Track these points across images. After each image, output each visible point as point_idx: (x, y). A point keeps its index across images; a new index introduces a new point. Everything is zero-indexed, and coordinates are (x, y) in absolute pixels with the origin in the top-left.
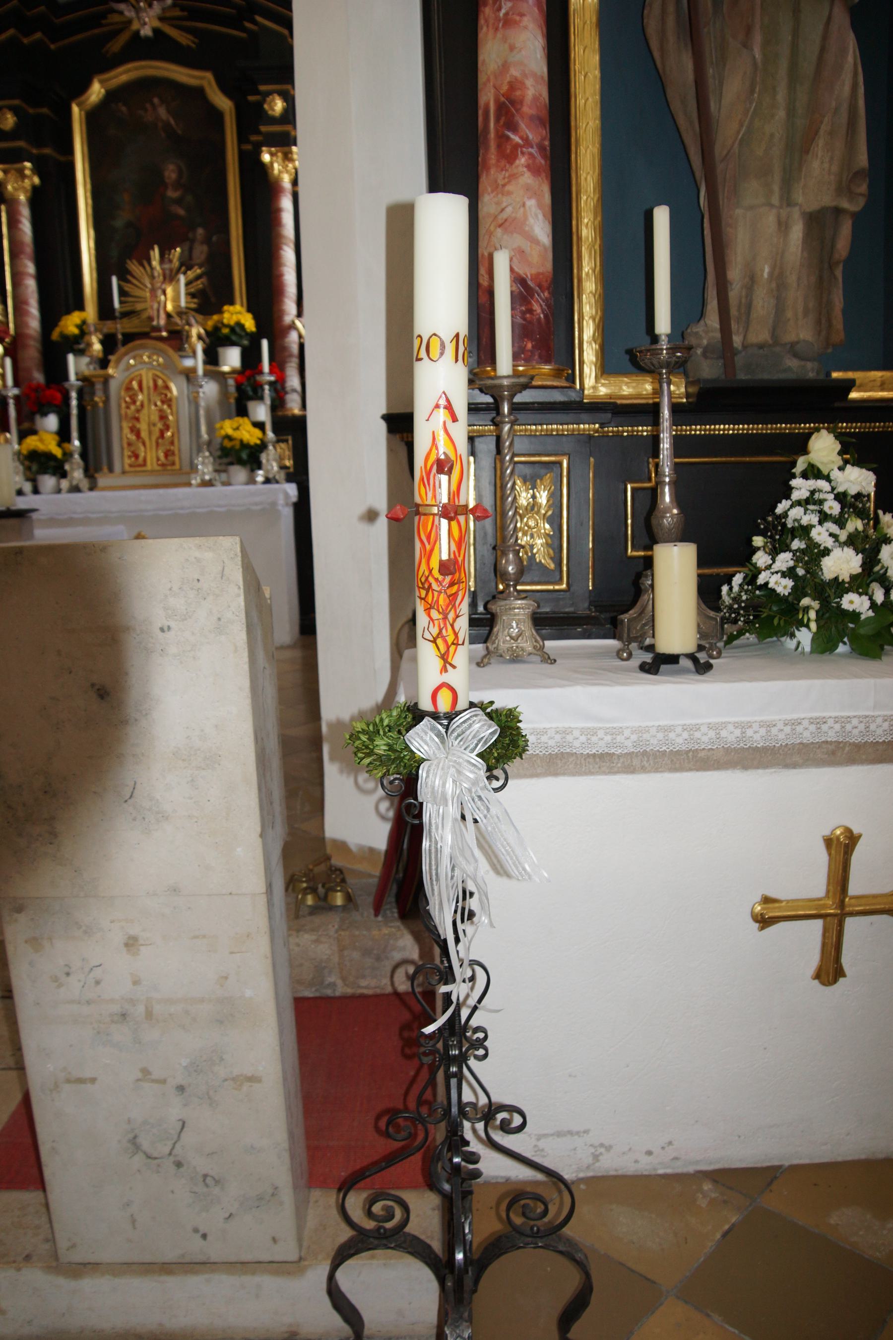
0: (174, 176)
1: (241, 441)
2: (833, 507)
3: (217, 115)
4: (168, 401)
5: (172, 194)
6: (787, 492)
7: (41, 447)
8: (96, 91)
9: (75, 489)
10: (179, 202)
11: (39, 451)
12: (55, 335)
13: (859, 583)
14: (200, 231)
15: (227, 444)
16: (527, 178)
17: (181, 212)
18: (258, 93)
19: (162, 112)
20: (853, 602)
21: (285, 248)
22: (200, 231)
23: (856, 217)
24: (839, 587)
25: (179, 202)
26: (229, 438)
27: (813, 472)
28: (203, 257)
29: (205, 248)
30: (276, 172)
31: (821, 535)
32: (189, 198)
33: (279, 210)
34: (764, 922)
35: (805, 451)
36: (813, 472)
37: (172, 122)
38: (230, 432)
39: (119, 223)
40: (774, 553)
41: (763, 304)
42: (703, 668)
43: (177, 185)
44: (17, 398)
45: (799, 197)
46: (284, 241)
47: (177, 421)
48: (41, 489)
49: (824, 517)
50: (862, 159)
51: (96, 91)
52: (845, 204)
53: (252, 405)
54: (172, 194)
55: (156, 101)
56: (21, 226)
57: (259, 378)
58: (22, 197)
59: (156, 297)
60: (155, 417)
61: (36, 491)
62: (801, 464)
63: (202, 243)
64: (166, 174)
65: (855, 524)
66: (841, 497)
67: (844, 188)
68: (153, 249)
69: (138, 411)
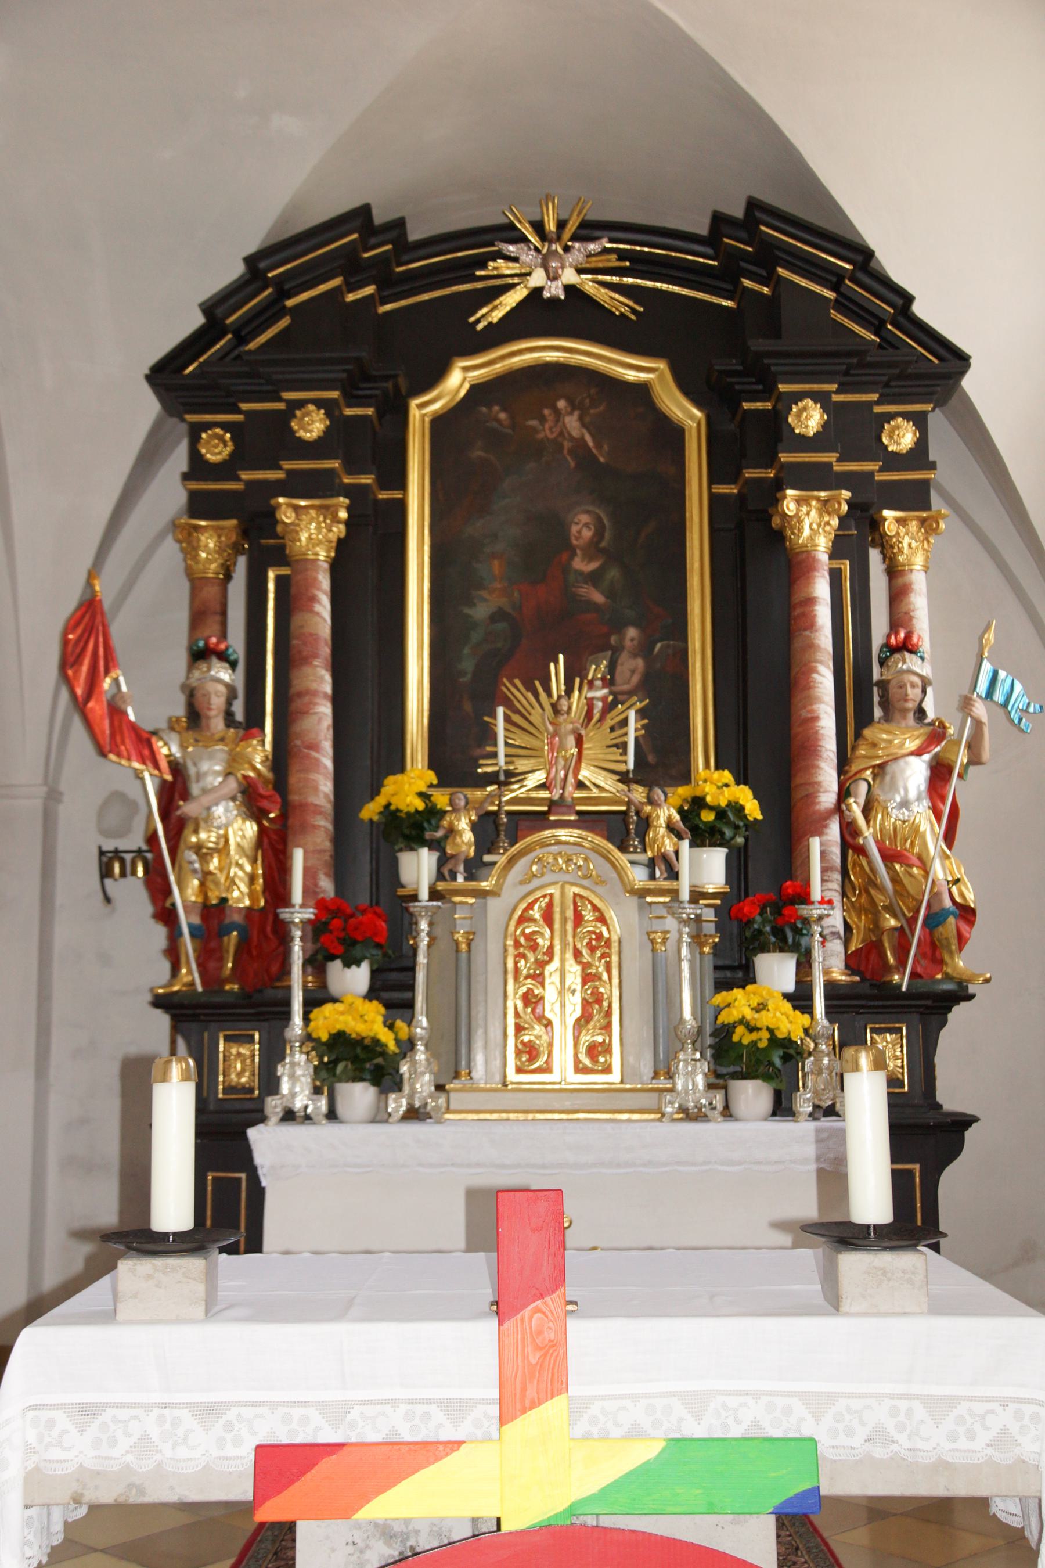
0: (587, 534)
1: (771, 1031)
3: (675, 434)
4: (599, 943)
5: (581, 565)
7: (355, 1027)
9: (413, 1114)
10: (594, 578)
11: (354, 1036)
12: (371, 811)
14: (632, 632)
15: (740, 1034)
17: (598, 598)
18: (768, 391)
19: (572, 423)
21: (821, 668)
22: (632, 632)
25: (594, 578)
28: (635, 679)
29: (640, 663)
30: (807, 532)
32: (614, 573)
33: (811, 601)
37: (588, 438)
38: (749, 1014)
39: (480, 612)
43: (593, 549)
46: (820, 656)
48: (341, 1110)
54: (581, 565)
55: (561, 404)
56: (317, 608)
57: (804, 910)
58: (323, 555)
59: (562, 747)
61: (332, 1115)
63: (635, 655)
64: (574, 529)
68: (556, 662)
69: (541, 964)
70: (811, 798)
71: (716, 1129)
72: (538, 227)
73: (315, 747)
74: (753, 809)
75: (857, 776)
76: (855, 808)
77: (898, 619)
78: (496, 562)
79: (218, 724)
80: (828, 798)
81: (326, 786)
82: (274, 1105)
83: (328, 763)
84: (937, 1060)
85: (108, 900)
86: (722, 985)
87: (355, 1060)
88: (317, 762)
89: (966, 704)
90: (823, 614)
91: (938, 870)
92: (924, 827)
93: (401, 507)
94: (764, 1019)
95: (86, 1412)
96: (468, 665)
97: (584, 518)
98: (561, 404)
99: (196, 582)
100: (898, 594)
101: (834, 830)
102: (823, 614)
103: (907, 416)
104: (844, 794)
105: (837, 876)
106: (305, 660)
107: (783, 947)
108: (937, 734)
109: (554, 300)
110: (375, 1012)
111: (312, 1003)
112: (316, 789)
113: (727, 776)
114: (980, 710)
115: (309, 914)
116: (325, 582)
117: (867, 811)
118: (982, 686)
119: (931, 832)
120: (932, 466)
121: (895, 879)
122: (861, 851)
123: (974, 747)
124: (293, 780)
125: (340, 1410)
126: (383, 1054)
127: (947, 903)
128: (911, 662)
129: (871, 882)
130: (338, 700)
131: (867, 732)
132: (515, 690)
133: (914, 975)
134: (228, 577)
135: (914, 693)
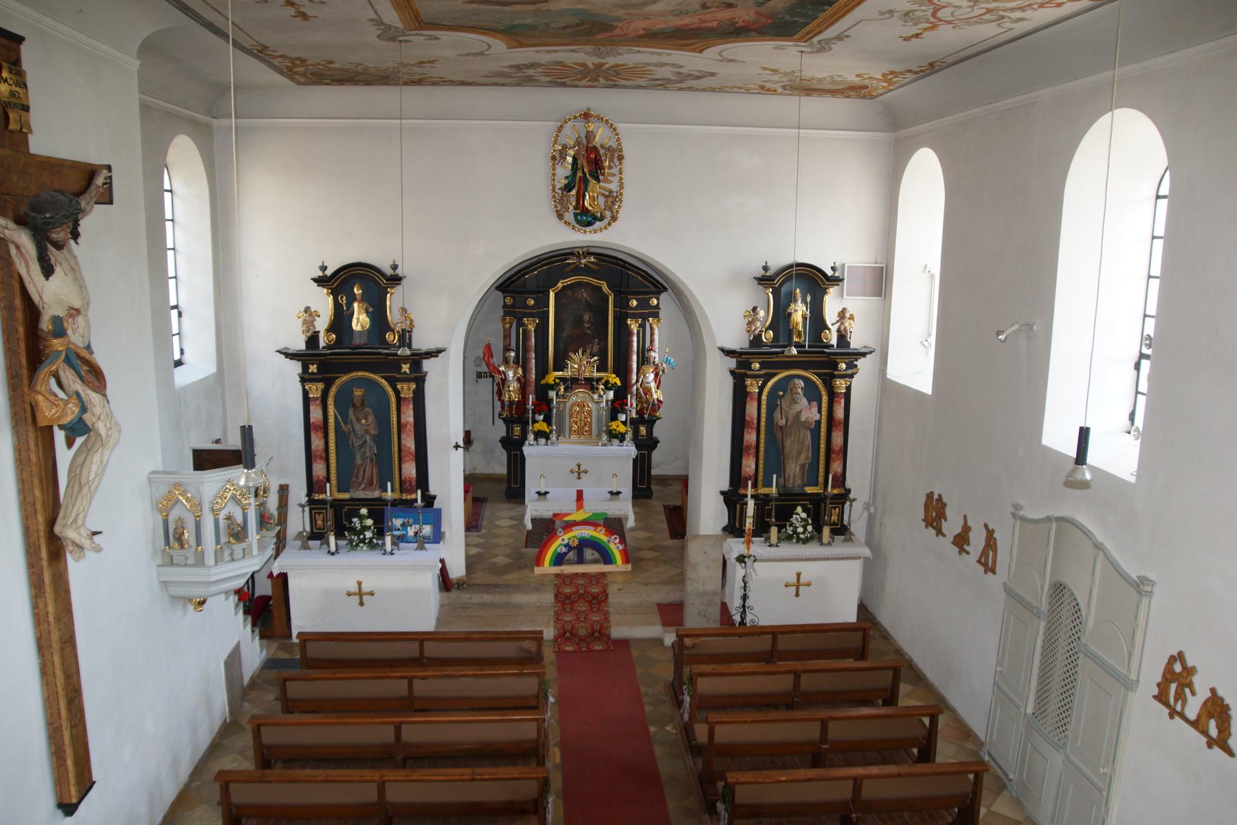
0: (588, 319)
2: (800, 520)
6: (792, 517)
7: (540, 428)
8: (560, 285)
9: (553, 444)
10: (589, 328)
12: (543, 382)
13: (803, 533)
14: (596, 340)
16: (752, 458)
17: (590, 332)
19: (585, 294)
20: (801, 536)
22: (596, 340)
23: (809, 464)
24: (800, 533)
25: (589, 328)
26: (615, 430)
27: (797, 514)
29: (598, 347)
31: (797, 525)
32: (593, 327)
33: (632, 341)
34: (786, 586)
35: (796, 509)
36: (797, 514)
38: (615, 427)
39: (565, 335)
40: (790, 527)
41: (791, 480)
42: (778, 546)
44: (532, 410)
45: (799, 463)
47: (591, 420)
49: (798, 521)
50: (810, 455)
51: (560, 285)
52: (807, 462)
53: (619, 415)
55: (583, 290)
60: (583, 418)
61: (538, 445)
62: (795, 512)
63: (597, 344)
65: (803, 523)
66: (801, 518)
67: (807, 459)
70: (630, 381)
71: (609, 448)
72: (579, 253)
73: (532, 369)
74: (619, 383)
75: (640, 377)
76: (639, 384)
77: (652, 341)
78: (568, 325)
79: (512, 363)
80: (634, 381)
81: (534, 377)
82: (527, 442)
83: (534, 372)
84: (654, 430)
85: (477, 381)
86: (612, 420)
87: (541, 434)
88: (532, 373)
89: (662, 364)
90: (635, 344)
91: (655, 396)
92: (653, 387)
93: (548, 311)
94: (618, 429)
95: (536, 510)
96: (562, 346)
97: (587, 315)
98: (583, 290)
99: (505, 330)
100: (652, 334)
101: (635, 388)
102: (635, 344)
103: (655, 298)
104: (637, 381)
105: (635, 397)
106: (530, 351)
107: (623, 413)
108: (657, 367)
109: (582, 267)
110: (545, 425)
111: (533, 423)
112: (531, 378)
113: (615, 376)
114: (664, 365)
115: (533, 407)
116: (533, 334)
117: (641, 385)
118: (665, 360)
119: (653, 385)
120: (660, 309)
121: (646, 397)
122: (640, 393)
123: (663, 371)
124: (527, 375)
125: (561, 510)
126: (547, 433)
127: (656, 402)
128: (653, 354)
129: (641, 397)
130: (536, 358)
131: (643, 367)
132: (572, 355)
133: (649, 414)
134: (511, 327)
135: (652, 360)
